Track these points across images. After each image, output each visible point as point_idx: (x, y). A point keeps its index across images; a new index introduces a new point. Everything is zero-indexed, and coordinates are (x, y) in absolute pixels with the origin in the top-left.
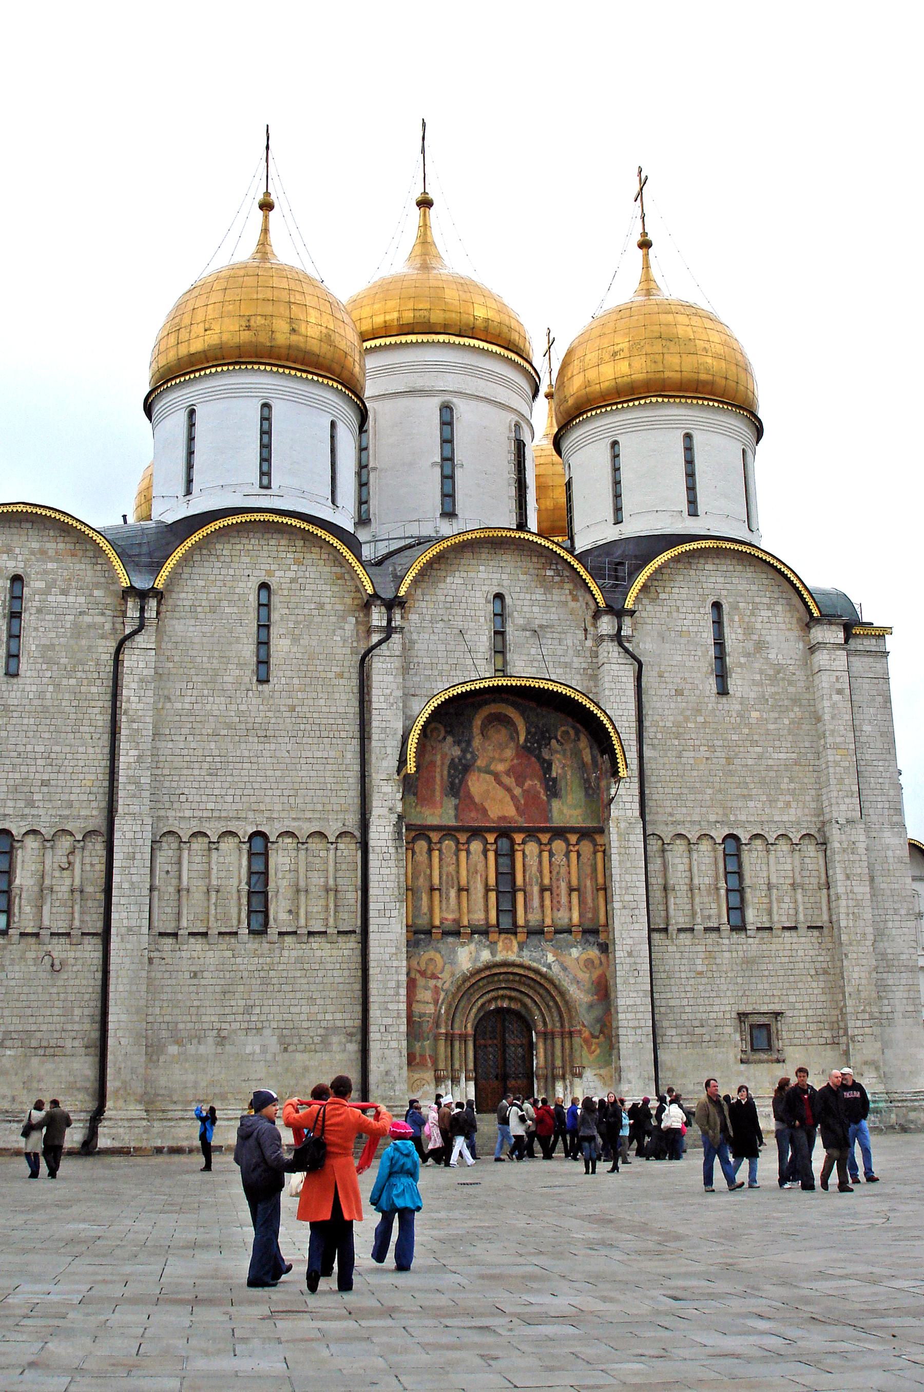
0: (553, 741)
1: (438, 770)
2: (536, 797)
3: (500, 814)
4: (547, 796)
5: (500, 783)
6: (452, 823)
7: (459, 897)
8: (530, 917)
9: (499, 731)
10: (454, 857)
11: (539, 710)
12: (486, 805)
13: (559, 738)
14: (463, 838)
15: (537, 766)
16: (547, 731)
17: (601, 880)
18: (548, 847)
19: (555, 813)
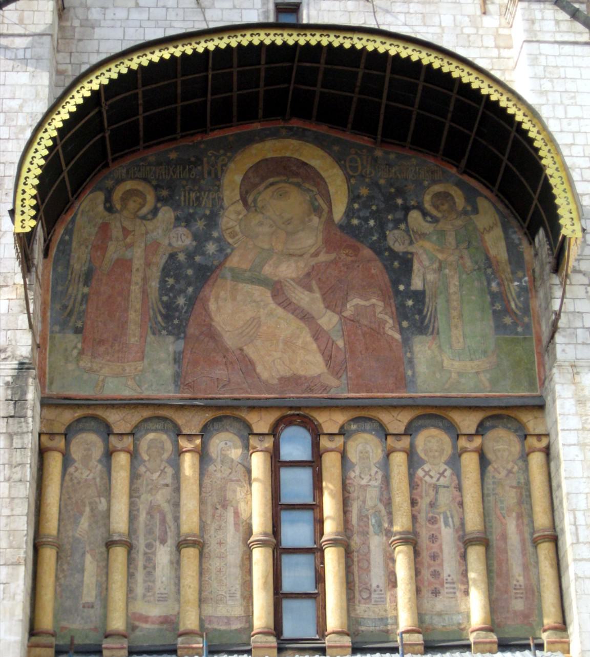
0: (414, 215)
1: (137, 278)
2: (375, 333)
3: (284, 371)
4: (402, 331)
5: (287, 304)
6: (167, 391)
7: (177, 564)
8: (361, 609)
9: (282, 195)
10: (170, 471)
11: (379, 153)
12: (250, 351)
13: (428, 206)
14: (191, 422)
15: (377, 268)
16: (400, 192)
17: (541, 520)
18: (405, 442)
19: (422, 368)
